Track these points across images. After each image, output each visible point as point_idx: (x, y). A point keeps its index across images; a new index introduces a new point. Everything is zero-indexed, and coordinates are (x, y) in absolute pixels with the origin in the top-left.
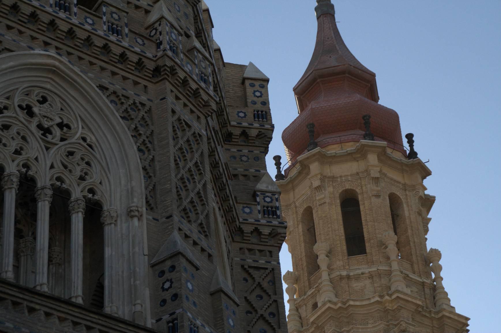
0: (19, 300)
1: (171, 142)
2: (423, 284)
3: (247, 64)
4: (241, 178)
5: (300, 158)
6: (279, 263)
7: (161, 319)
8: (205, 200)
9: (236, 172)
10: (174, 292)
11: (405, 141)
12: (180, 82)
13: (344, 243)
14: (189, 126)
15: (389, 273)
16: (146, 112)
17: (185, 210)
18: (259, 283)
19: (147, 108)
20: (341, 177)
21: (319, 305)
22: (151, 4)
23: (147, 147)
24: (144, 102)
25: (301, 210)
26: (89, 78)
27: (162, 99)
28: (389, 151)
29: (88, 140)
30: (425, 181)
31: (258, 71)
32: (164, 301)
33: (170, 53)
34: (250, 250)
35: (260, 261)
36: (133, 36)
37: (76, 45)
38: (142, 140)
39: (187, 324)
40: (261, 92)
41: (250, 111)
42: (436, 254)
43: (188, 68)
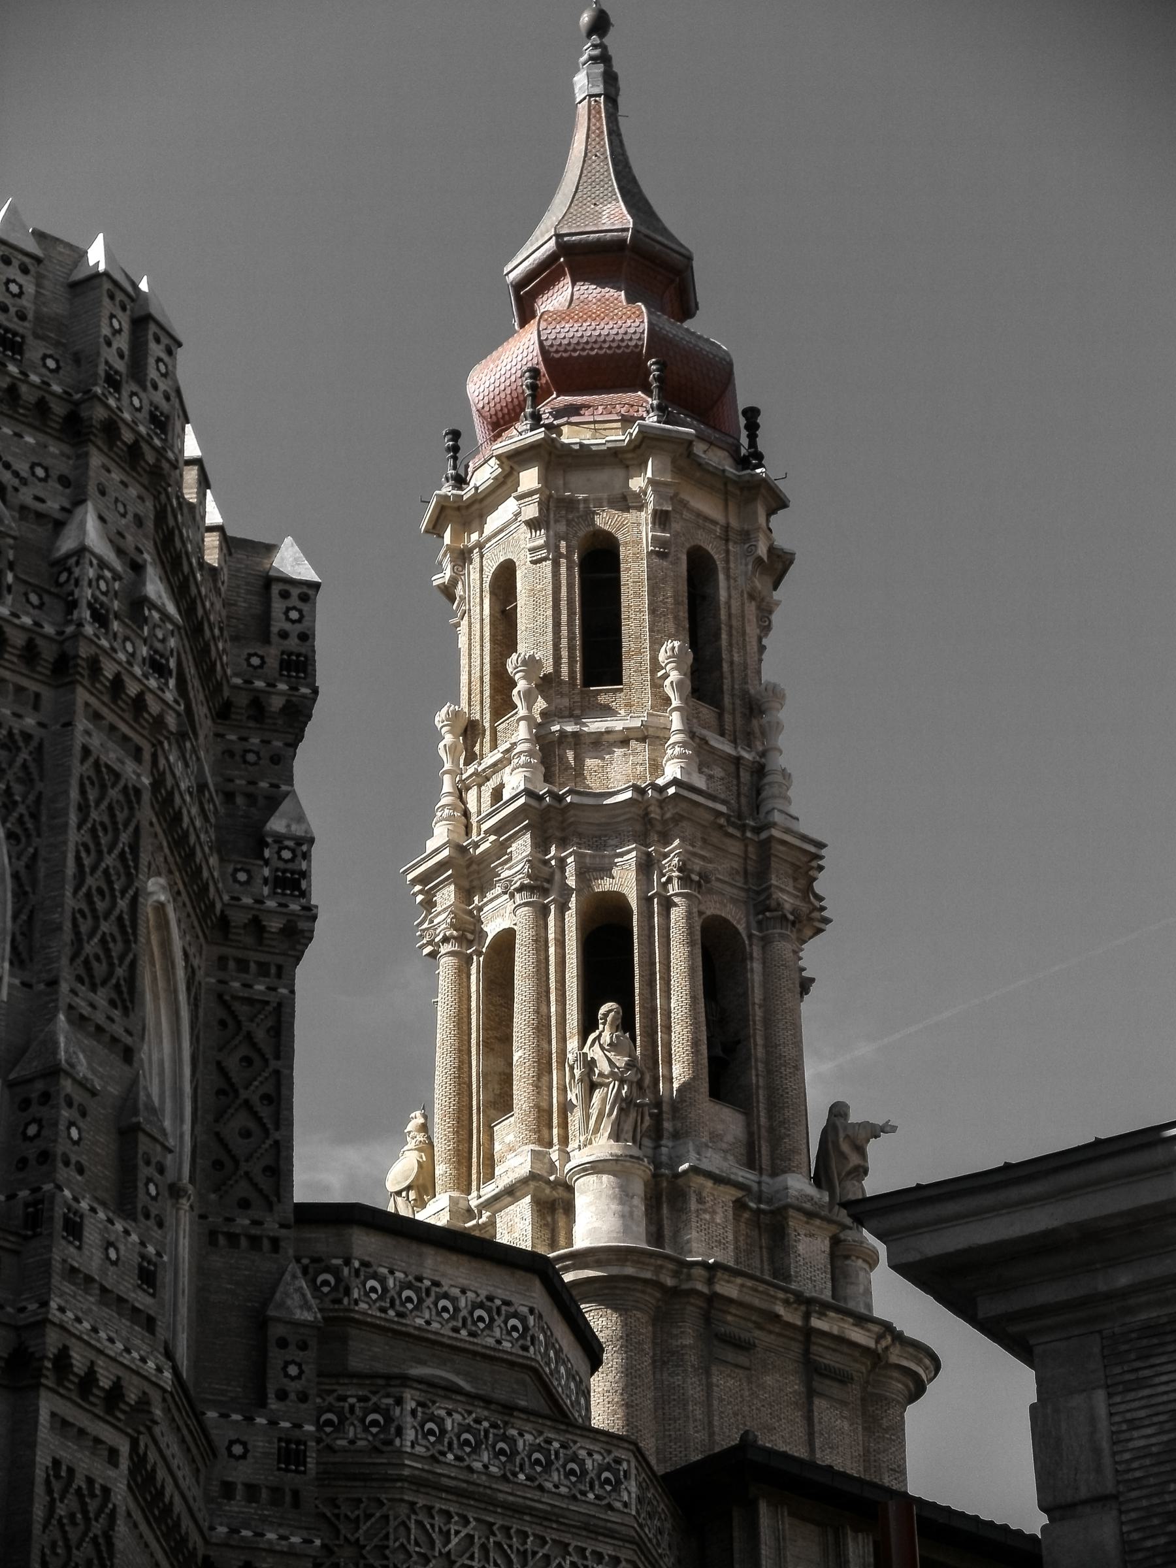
1: (73, 819)
2: (737, 761)
6: (293, 992)
9: (230, 787)
14: (117, 776)
19: (34, 743)
22: (67, 506)
24: (30, 731)
25: (491, 567)
28: (699, 449)
30: (773, 518)
32: (23, 1163)
36: (21, 588)
38: (15, 815)
39: (59, 1211)
40: (300, 611)
41: (273, 654)
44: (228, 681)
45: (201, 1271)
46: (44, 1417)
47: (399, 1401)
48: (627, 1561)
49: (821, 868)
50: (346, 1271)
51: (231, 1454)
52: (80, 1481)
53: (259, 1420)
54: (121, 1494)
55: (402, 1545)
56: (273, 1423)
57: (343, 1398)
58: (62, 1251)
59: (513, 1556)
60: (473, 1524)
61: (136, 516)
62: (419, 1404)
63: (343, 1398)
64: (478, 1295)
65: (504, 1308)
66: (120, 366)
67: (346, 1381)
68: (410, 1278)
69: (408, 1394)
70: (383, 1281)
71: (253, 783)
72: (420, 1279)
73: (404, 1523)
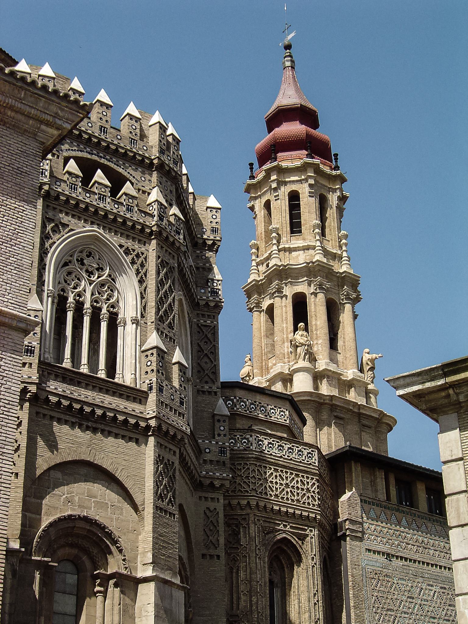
0: (73, 378)
4: (201, 270)
6: (218, 323)
7: (145, 382)
10: (152, 368)
18: (206, 335)
19: (144, 256)
21: (270, 266)
26: (114, 240)
28: (321, 166)
29: (112, 276)
32: (147, 372)
37: (108, 222)
44: (197, 236)
45: (195, 402)
47: (251, 436)
49: (359, 283)
50: (235, 400)
53: (213, 442)
55: (254, 476)
56: (217, 443)
57: (236, 436)
61: (170, 191)
63: (236, 436)
66: (164, 148)
70: (245, 402)
71: (204, 265)
72: (255, 402)
73: (254, 470)
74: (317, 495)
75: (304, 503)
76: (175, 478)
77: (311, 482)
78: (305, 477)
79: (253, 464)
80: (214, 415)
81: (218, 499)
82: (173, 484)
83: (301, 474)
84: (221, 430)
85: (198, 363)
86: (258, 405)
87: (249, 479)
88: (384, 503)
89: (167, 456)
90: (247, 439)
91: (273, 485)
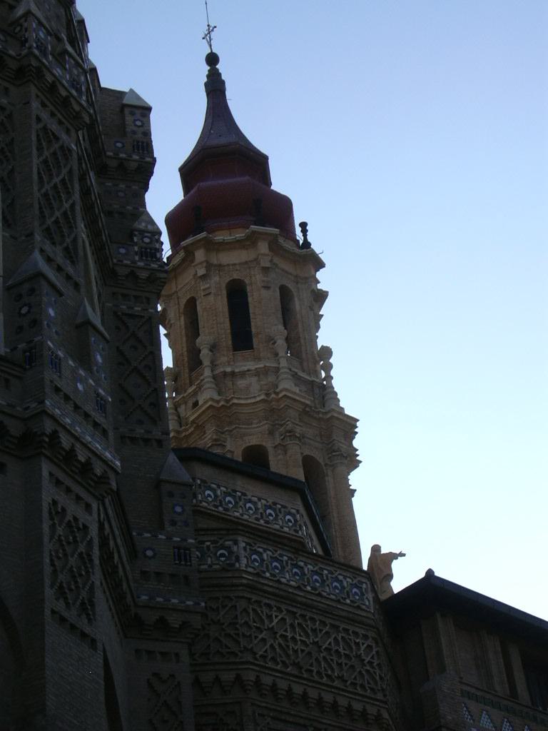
1: (35, 151)
3: (126, 90)
5: (183, 243)
8: (72, 222)
11: (298, 230)
12: (47, 86)
13: (230, 337)
14: (57, 139)
15: (277, 370)
16: (5, 117)
17: (48, 229)
20: (228, 265)
21: (200, 403)
23: (6, 157)
25: (183, 301)
27: (25, 104)
28: (281, 240)
30: (318, 273)
31: (139, 98)
32: (21, 328)
33: (36, 52)
34: (124, 295)
35: (136, 308)
42: (327, 352)
43: (58, 71)
44: (105, 154)
46: (45, 473)
47: (236, 543)
48: (373, 638)
51: (146, 556)
52: (69, 517)
54: (94, 531)
56: (169, 538)
58: (49, 375)
59: (309, 631)
60: (285, 612)
62: (247, 544)
64: (268, 502)
65: (282, 510)
67: (203, 533)
68: (229, 490)
69: (240, 538)
74: (378, 672)
75: (354, 684)
76: (91, 561)
77: (363, 644)
78: (350, 632)
79: (243, 597)
80: (158, 483)
81: (177, 655)
82: (87, 572)
83: (343, 626)
84: (175, 512)
85: (120, 385)
86: (240, 498)
87: (237, 629)
88: (506, 702)
89: (73, 510)
90: (228, 549)
91: (288, 644)
